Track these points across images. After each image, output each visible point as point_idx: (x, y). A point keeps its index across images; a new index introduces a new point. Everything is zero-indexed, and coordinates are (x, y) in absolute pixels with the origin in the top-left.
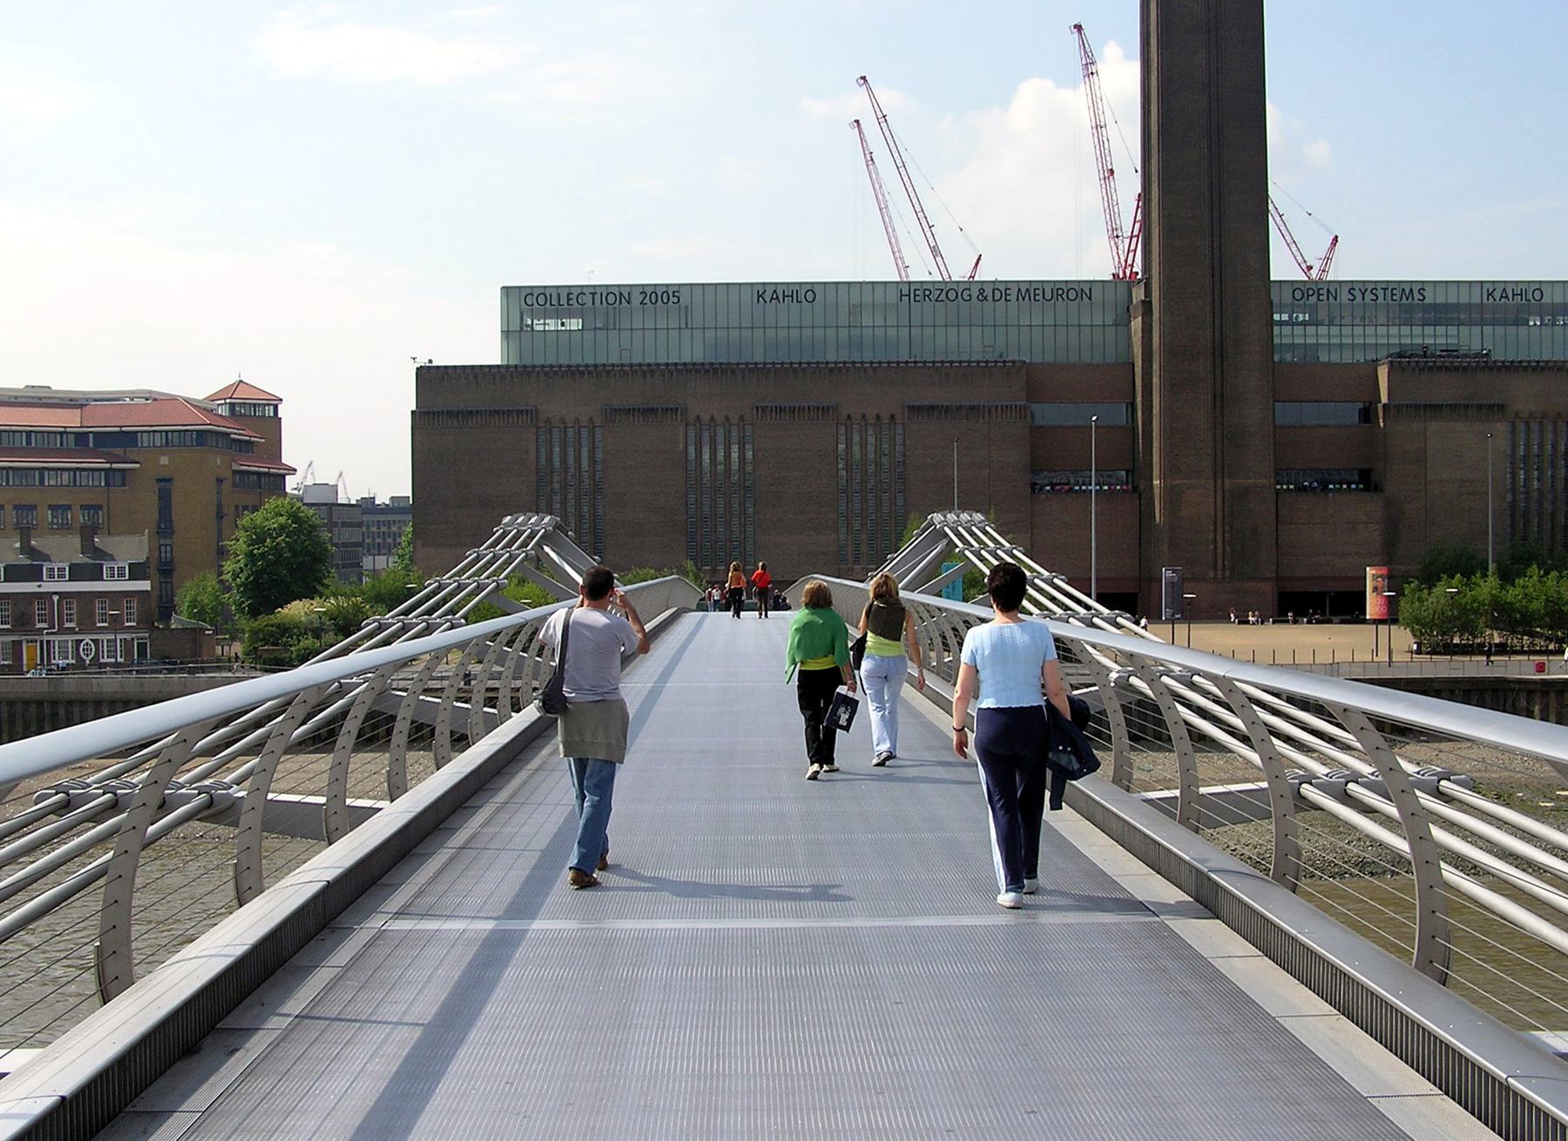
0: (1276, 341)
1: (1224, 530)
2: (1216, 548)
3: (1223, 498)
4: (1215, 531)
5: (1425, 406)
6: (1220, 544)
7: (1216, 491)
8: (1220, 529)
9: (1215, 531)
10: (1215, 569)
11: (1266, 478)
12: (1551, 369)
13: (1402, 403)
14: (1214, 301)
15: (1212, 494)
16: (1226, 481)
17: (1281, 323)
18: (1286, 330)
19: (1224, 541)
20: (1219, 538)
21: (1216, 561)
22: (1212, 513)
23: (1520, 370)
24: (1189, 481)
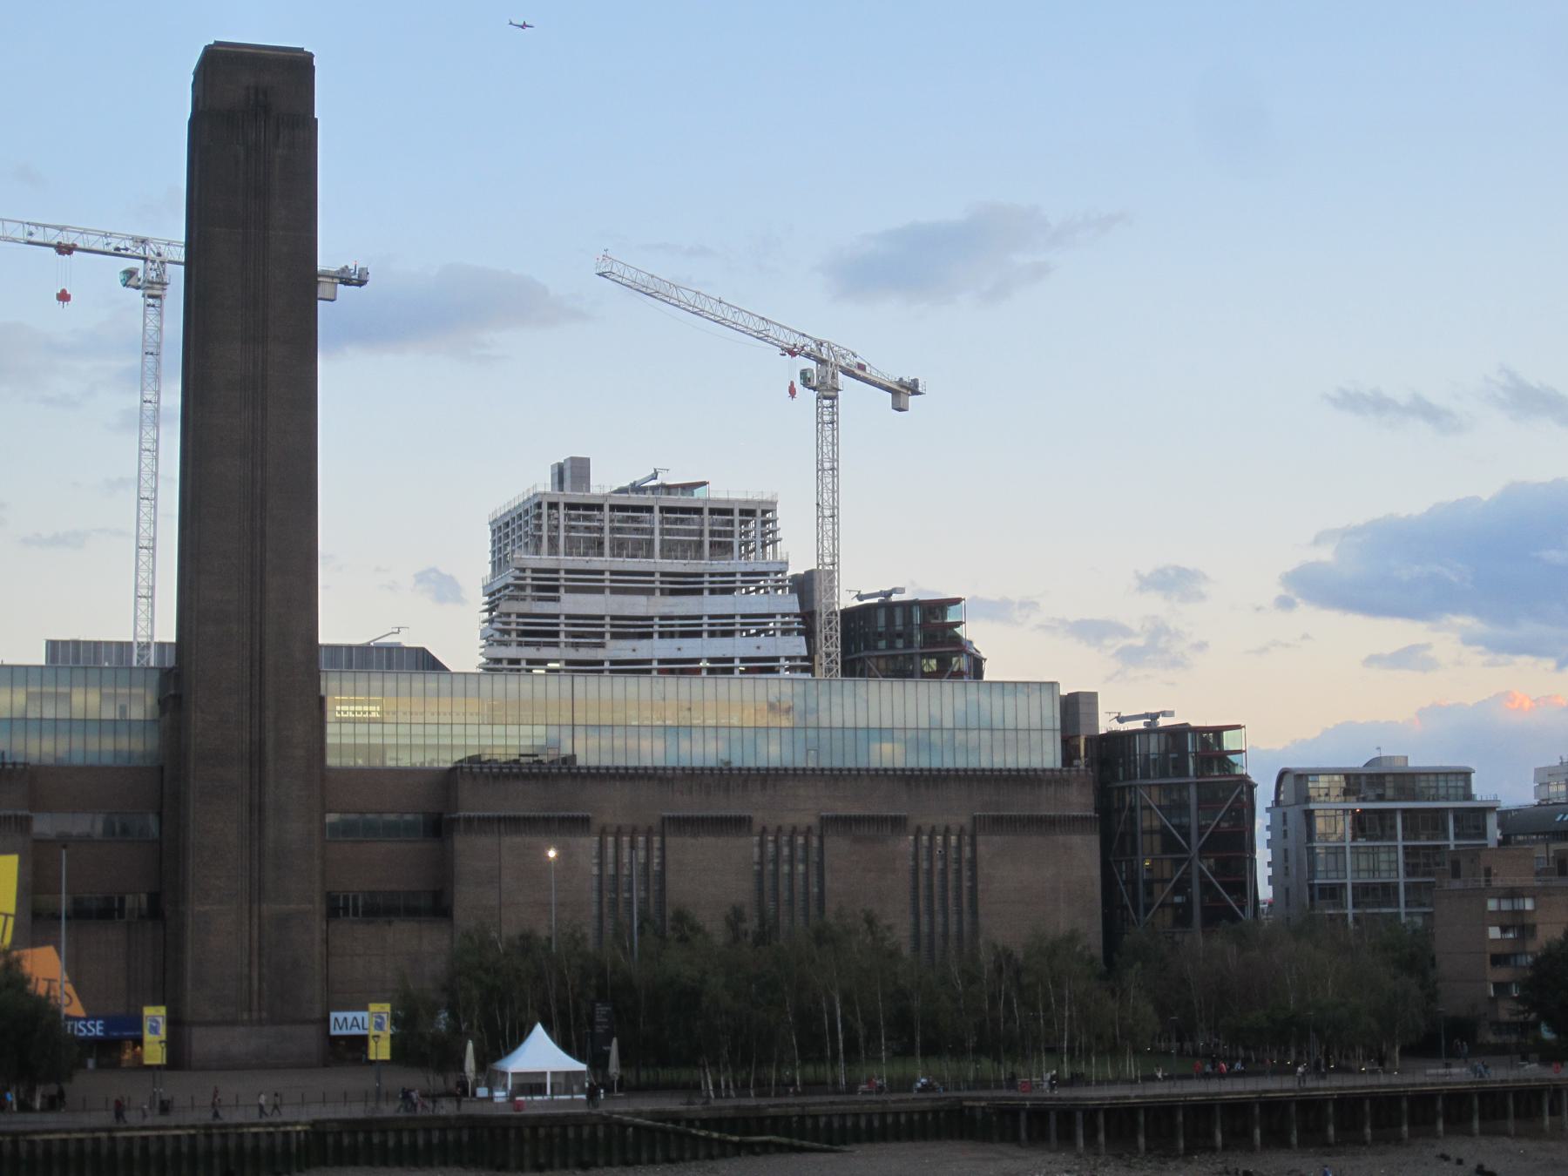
0: (330, 740)
7: (251, 918)
8: (255, 959)
9: (250, 964)
10: (250, 1010)
12: (641, 777)
13: (472, 814)
16: (264, 906)
17: (341, 721)
18: (348, 728)
20: (255, 975)
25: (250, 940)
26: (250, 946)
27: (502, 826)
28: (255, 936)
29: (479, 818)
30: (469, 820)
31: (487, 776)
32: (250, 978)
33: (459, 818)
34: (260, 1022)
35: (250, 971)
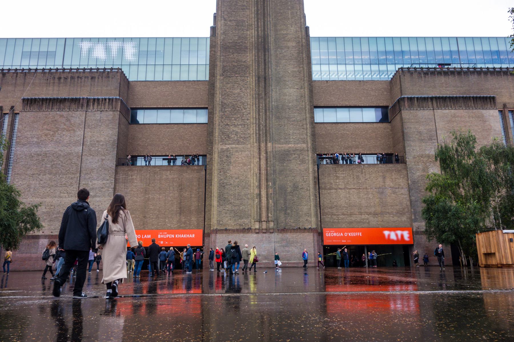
1: (267, 186)
2: (260, 201)
3: (267, 160)
4: (260, 187)
5: (432, 98)
6: (264, 199)
7: (260, 154)
8: (263, 182)
9: (260, 187)
10: (260, 221)
11: (304, 143)
14: (258, 10)
15: (256, 155)
16: (269, 145)
19: (267, 195)
21: (260, 215)
22: (256, 170)
23: (502, 73)
24: (237, 146)
25: (260, 170)
26: (260, 173)
27: (435, 103)
28: (263, 166)
29: (417, 98)
30: (411, 99)
31: (419, 73)
32: (259, 195)
33: (404, 98)
34: (267, 231)
35: (260, 191)
